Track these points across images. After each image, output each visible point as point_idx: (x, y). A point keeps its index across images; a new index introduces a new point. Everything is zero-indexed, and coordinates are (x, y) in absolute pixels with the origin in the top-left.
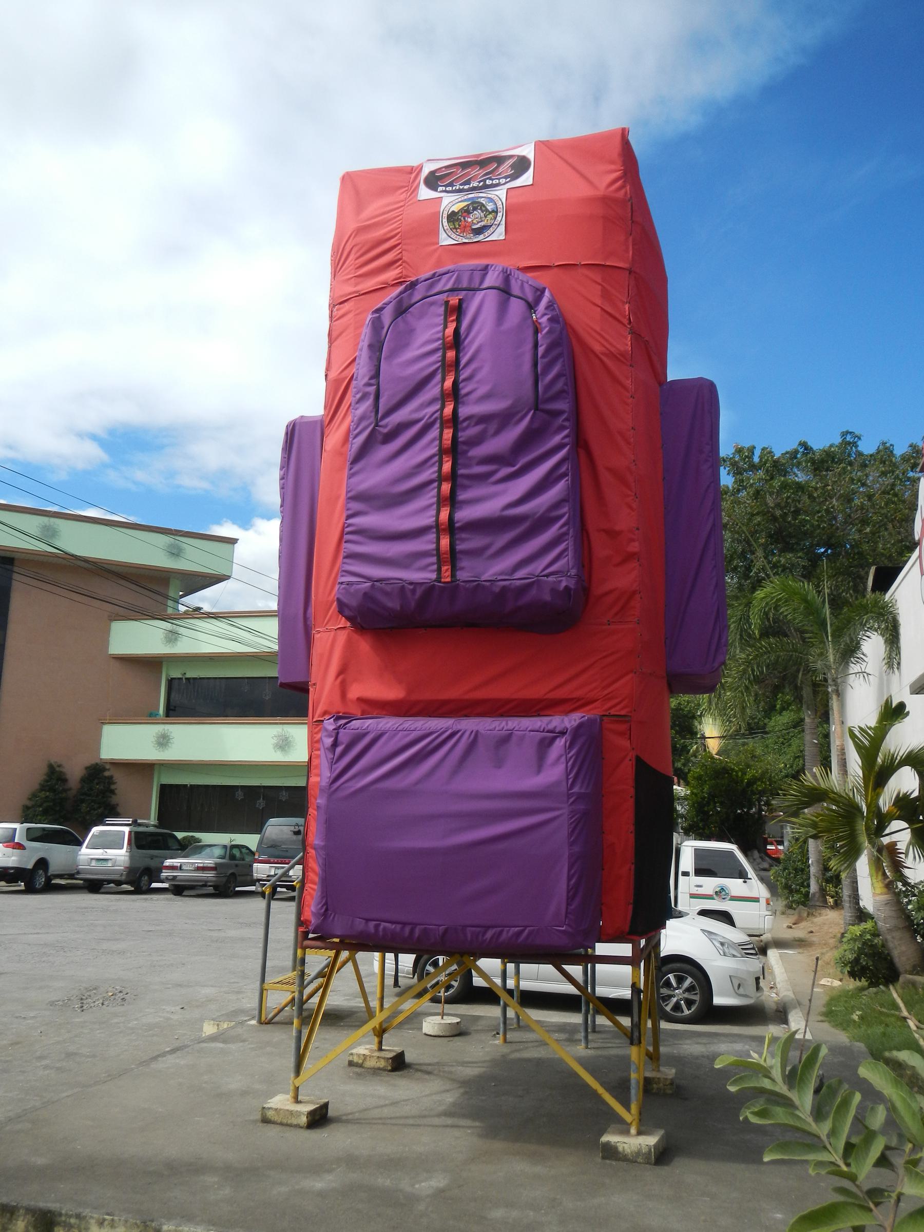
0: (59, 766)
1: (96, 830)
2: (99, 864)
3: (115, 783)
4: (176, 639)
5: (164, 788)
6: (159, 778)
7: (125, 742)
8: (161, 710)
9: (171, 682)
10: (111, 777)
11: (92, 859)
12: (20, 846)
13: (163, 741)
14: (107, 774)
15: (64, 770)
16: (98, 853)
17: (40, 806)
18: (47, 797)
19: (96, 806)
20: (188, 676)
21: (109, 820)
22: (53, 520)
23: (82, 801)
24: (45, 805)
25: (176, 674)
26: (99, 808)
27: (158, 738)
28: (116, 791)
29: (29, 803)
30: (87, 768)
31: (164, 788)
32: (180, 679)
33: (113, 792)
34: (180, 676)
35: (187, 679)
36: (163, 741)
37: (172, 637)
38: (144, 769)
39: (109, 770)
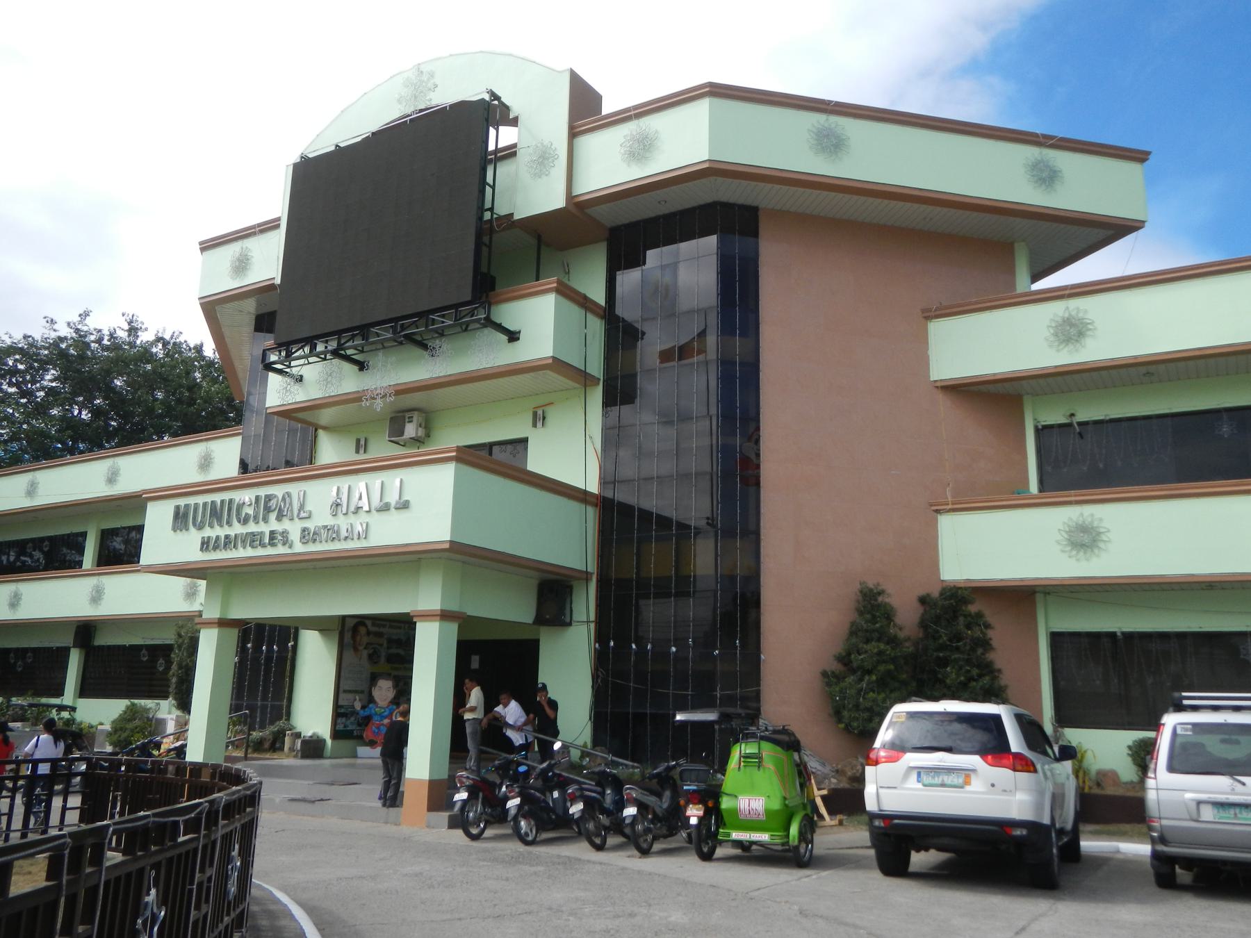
0: (881, 593)
1: (1171, 720)
2: (1227, 816)
3: (988, 626)
4: (1081, 334)
5: (1057, 639)
6: (1046, 623)
7: (995, 545)
8: (1034, 487)
9: (1041, 431)
10: (979, 615)
11: (1199, 803)
12: (1022, 764)
13: (1084, 540)
14: (972, 609)
15: (887, 600)
16: (1218, 786)
17: (869, 672)
18: (880, 653)
19: (975, 672)
20: (1084, 415)
21: (1190, 697)
22: (835, 120)
23: (944, 663)
24: (882, 668)
25: (1055, 417)
26: (980, 676)
27: (1069, 532)
28: (994, 643)
29: (835, 667)
30: (923, 600)
31: (1057, 639)
32: (1061, 426)
33: (986, 644)
34: (1063, 420)
35: (1080, 424)
36: (1084, 540)
37: (1072, 331)
38: (1021, 597)
39: (971, 602)
